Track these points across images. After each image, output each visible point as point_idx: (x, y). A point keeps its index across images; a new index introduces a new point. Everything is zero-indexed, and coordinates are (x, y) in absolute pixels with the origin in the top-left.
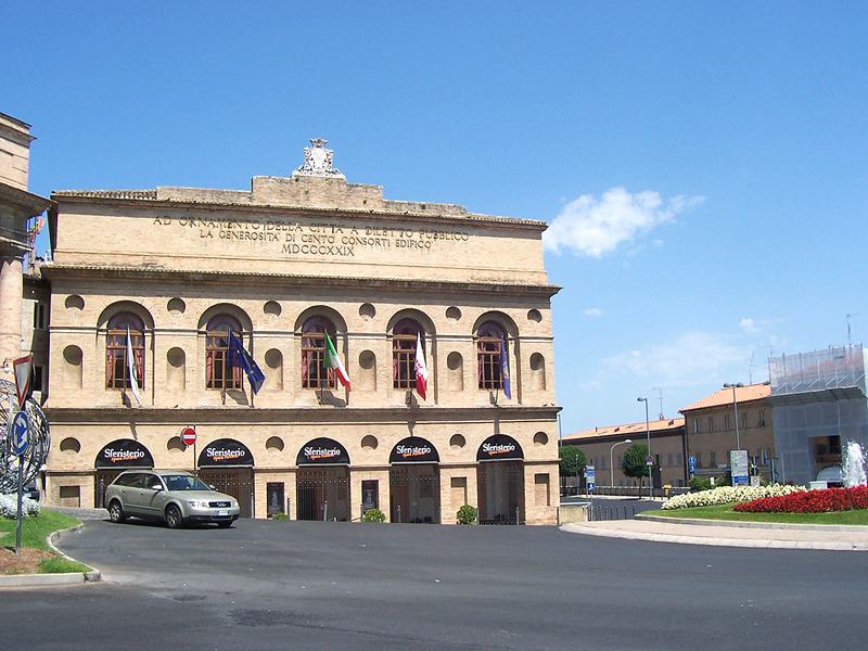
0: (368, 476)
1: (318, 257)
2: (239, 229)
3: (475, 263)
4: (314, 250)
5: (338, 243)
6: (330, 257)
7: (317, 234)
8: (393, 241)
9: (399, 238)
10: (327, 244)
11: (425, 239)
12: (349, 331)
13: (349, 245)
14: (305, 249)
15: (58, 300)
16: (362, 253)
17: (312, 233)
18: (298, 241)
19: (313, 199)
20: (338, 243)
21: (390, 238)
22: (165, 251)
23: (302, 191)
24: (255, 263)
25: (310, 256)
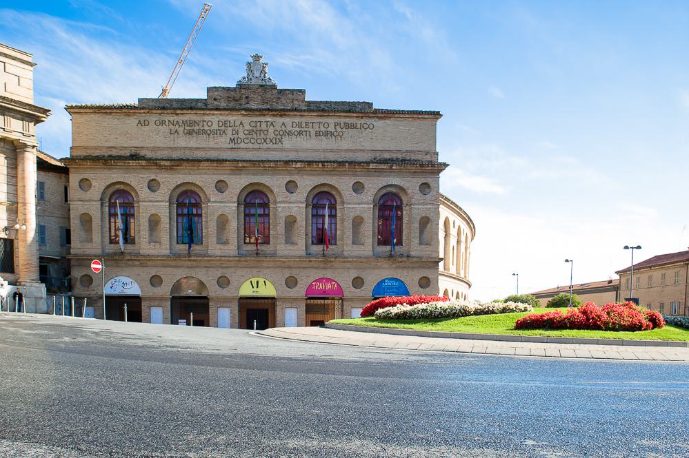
2: (196, 128)
3: (379, 147)
4: (253, 141)
5: (271, 135)
6: (265, 146)
7: (255, 129)
8: (313, 133)
10: (262, 135)
12: (278, 200)
14: (246, 141)
15: (74, 179)
16: (288, 143)
17: (251, 128)
18: (241, 135)
20: (271, 135)
22: (146, 145)
24: (209, 153)
25: (250, 146)
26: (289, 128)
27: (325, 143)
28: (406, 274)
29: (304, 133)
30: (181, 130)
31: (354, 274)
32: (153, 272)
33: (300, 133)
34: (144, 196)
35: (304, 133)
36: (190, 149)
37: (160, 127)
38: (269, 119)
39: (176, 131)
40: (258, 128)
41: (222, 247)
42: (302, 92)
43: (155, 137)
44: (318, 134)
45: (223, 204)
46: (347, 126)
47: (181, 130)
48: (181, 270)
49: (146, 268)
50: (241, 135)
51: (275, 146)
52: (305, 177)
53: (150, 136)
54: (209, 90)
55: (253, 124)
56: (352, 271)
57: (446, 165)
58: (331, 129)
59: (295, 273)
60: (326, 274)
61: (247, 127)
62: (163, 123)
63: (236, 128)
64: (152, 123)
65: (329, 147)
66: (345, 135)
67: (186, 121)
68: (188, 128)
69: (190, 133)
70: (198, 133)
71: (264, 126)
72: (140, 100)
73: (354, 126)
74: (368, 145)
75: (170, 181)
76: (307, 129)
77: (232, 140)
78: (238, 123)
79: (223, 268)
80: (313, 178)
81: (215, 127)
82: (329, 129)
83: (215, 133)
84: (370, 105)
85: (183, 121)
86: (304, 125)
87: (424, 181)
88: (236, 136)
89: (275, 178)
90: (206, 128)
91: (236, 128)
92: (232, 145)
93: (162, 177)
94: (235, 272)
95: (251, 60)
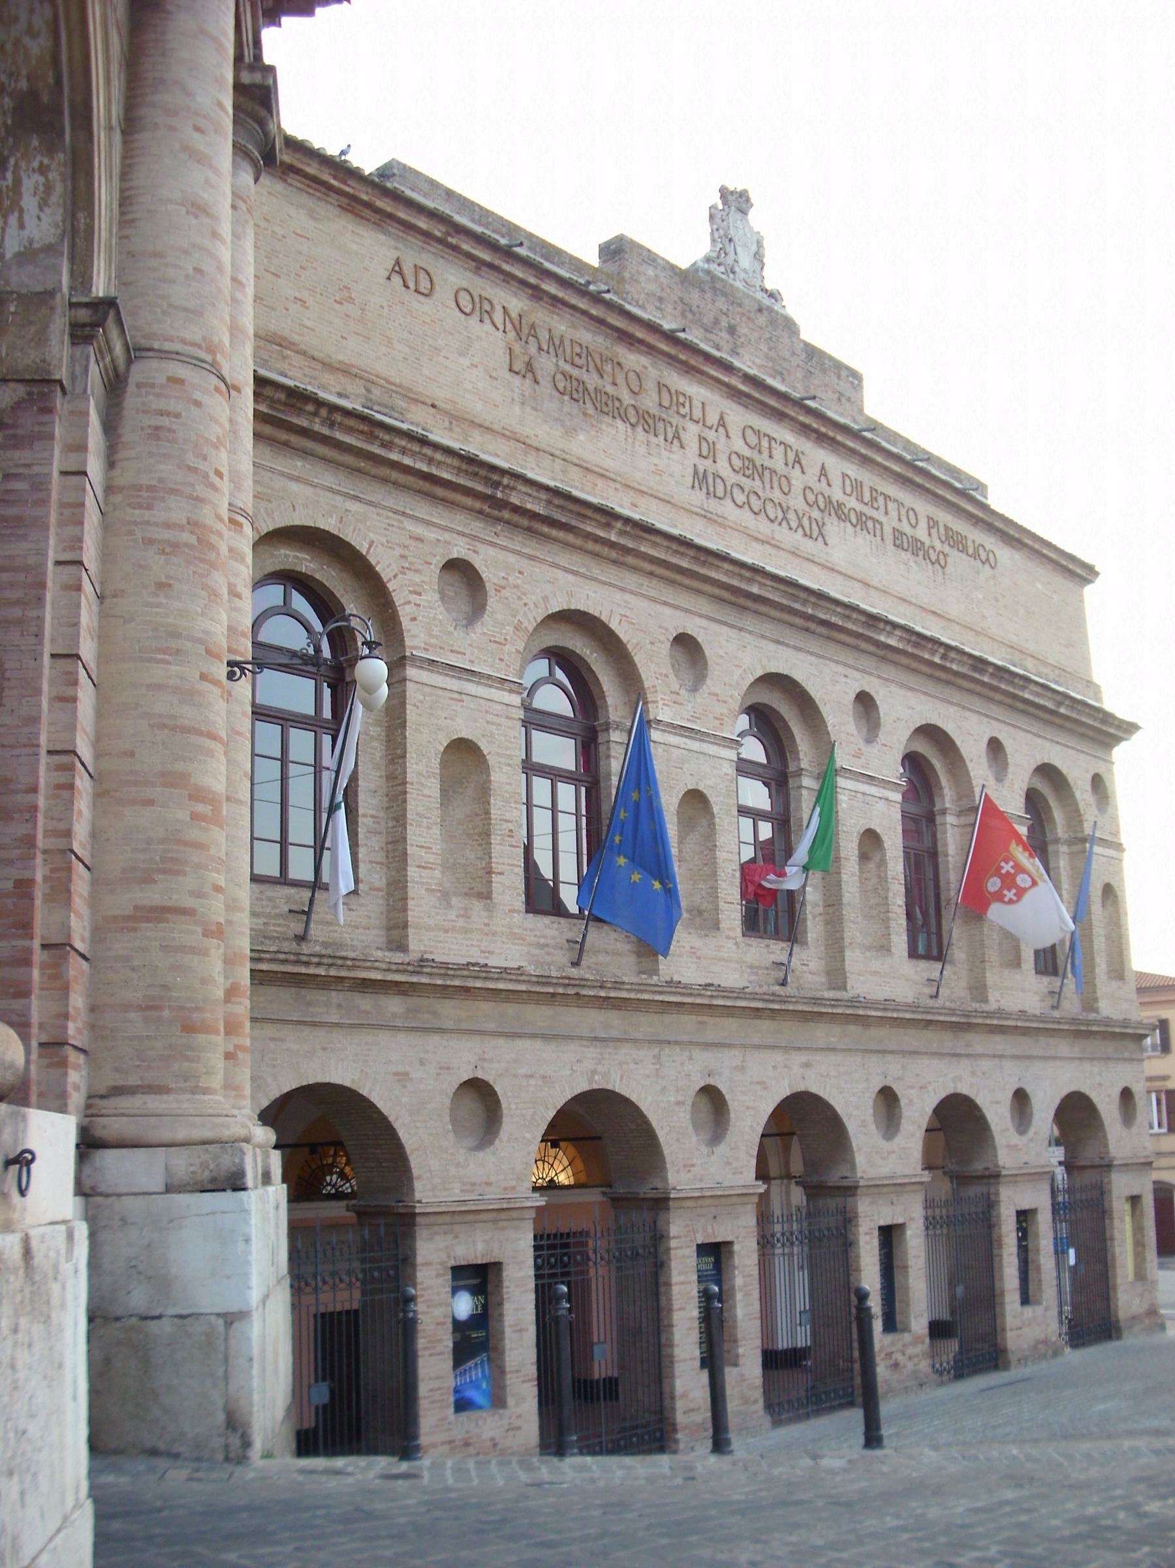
4: (756, 504)
5: (796, 502)
6: (784, 535)
8: (888, 531)
10: (777, 495)
13: (816, 514)
23: (724, 323)
24: (643, 501)
29: (870, 524)
32: (464, 1058)
33: (862, 522)
34: (423, 636)
35: (870, 524)
37: (474, 321)
44: (901, 541)
45: (695, 745)
47: (546, 364)
48: (571, 1052)
52: (893, 688)
53: (438, 350)
56: (1008, 1065)
57: (1129, 728)
58: (921, 533)
60: (959, 1078)
66: (950, 569)
67: (562, 341)
69: (575, 392)
71: (778, 452)
78: (712, 419)
79: (708, 1046)
84: (981, 487)
85: (551, 338)
89: (830, 669)
90: (627, 399)
91: (711, 435)
93: (497, 557)
94: (742, 1069)
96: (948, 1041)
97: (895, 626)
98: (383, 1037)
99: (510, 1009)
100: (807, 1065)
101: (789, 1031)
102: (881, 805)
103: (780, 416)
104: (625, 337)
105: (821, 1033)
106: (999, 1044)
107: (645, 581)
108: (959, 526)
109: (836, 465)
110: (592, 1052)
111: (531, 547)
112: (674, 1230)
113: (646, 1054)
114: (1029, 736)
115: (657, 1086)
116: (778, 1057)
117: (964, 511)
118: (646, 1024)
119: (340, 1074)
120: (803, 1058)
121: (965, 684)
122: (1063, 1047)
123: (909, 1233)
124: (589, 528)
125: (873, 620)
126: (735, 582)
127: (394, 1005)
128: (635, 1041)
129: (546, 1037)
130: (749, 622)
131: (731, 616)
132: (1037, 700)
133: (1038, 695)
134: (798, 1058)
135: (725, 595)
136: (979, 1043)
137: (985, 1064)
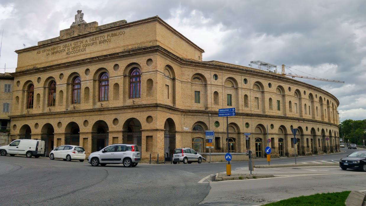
0: (85, 137)
1: (76, 54)
2: (56, 50)
5: (82, 48)
6: (79, 53)
8: (98, 42)
9: (100, 40)
11: (109, 38)
16: (88, 50)
17: (74, 46)
19: (75, 34)
20: (82, 48)
21: (97, 41)
23: (72, 31)
24: (58, 61)
25: (74, 54)
26: (89, 42)
27: (104, 46)
28: (140, 115)
30: (50, 53)
31: (113, 117)
32: (36, 121)
33: (93, 44)
36: (52, 61)
38: (81, 40)
39: (49, 54)
40: (77, 45)
41: (60, 107)
42: (95, 23)
43: (42, 59)
44: (100, 43)
45: (61, 86)
46: (113, 35)
48: (45, 120)
49: (34, 120)
50: (71, 50)
51: (83, 53)
54: (61, 32)
55: (75, 44)
56: (113, 115)
58: (106, 38)
59: (87, 118)
61: (73, 46)
62: (45, 51)
63: (69, 47)
64: (41, 52)
65: (105, 48)
66: (112, 40)
68: (53, 51)
70: (56, 53)
72: (39, 43)
73: (115, 35)
74: (122, 44)
75: (44, 76)
76: (96, 41)
77: (67, 54)
78: (70, 45)
80: (96, 66)
81: (62, 48)
82: (105, 39)
83: (61, 51)
86: (94, 39)
87: (148, 58)
88: (69, 51)
92: (67, 56)
95: (77, 13)
96: (99, 113)
97: (87, 59)
98: (30, 120)
99: (40, 117)
100: (73, 119)
101: (71, 115)
102: (89, 83)
103: (79, 38)
104: (58, 44)
105: (75, 115)
106: (111, 112)
107: (57, 70)
108: (113, 32)
109: (88, 39)
110: (47, 120)
111: (45, 73)
112: (54, 137)
113: (53, 119)
114: (126, 60)
115: (53, 122)
116: (69, 118)
117: (114, 29)
118: (53, 116)
119: (27, 124)
120: (73, 118)
121: (107, 59)
122: (129, 111)
123: (88, 139)
124: (48, 69)
125: (83, 60)
126: (64, 65)
127: (31, 118)
128: (52, 118)
129: (43, 119)
130: (69, 68)
131: (66, 69)
132: (123, 55)
133: (122, 54)
134: (72, 118)
135: (66, 67)
136: (106, 113)
137: (107, 116)
